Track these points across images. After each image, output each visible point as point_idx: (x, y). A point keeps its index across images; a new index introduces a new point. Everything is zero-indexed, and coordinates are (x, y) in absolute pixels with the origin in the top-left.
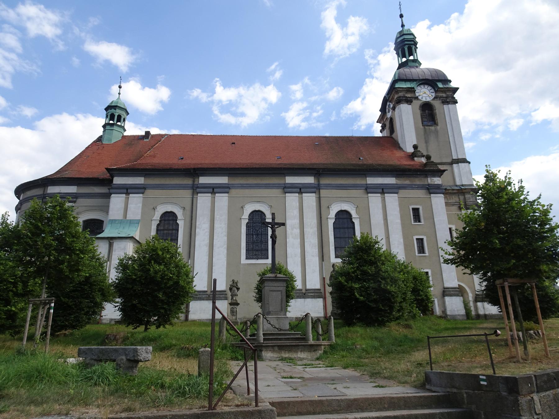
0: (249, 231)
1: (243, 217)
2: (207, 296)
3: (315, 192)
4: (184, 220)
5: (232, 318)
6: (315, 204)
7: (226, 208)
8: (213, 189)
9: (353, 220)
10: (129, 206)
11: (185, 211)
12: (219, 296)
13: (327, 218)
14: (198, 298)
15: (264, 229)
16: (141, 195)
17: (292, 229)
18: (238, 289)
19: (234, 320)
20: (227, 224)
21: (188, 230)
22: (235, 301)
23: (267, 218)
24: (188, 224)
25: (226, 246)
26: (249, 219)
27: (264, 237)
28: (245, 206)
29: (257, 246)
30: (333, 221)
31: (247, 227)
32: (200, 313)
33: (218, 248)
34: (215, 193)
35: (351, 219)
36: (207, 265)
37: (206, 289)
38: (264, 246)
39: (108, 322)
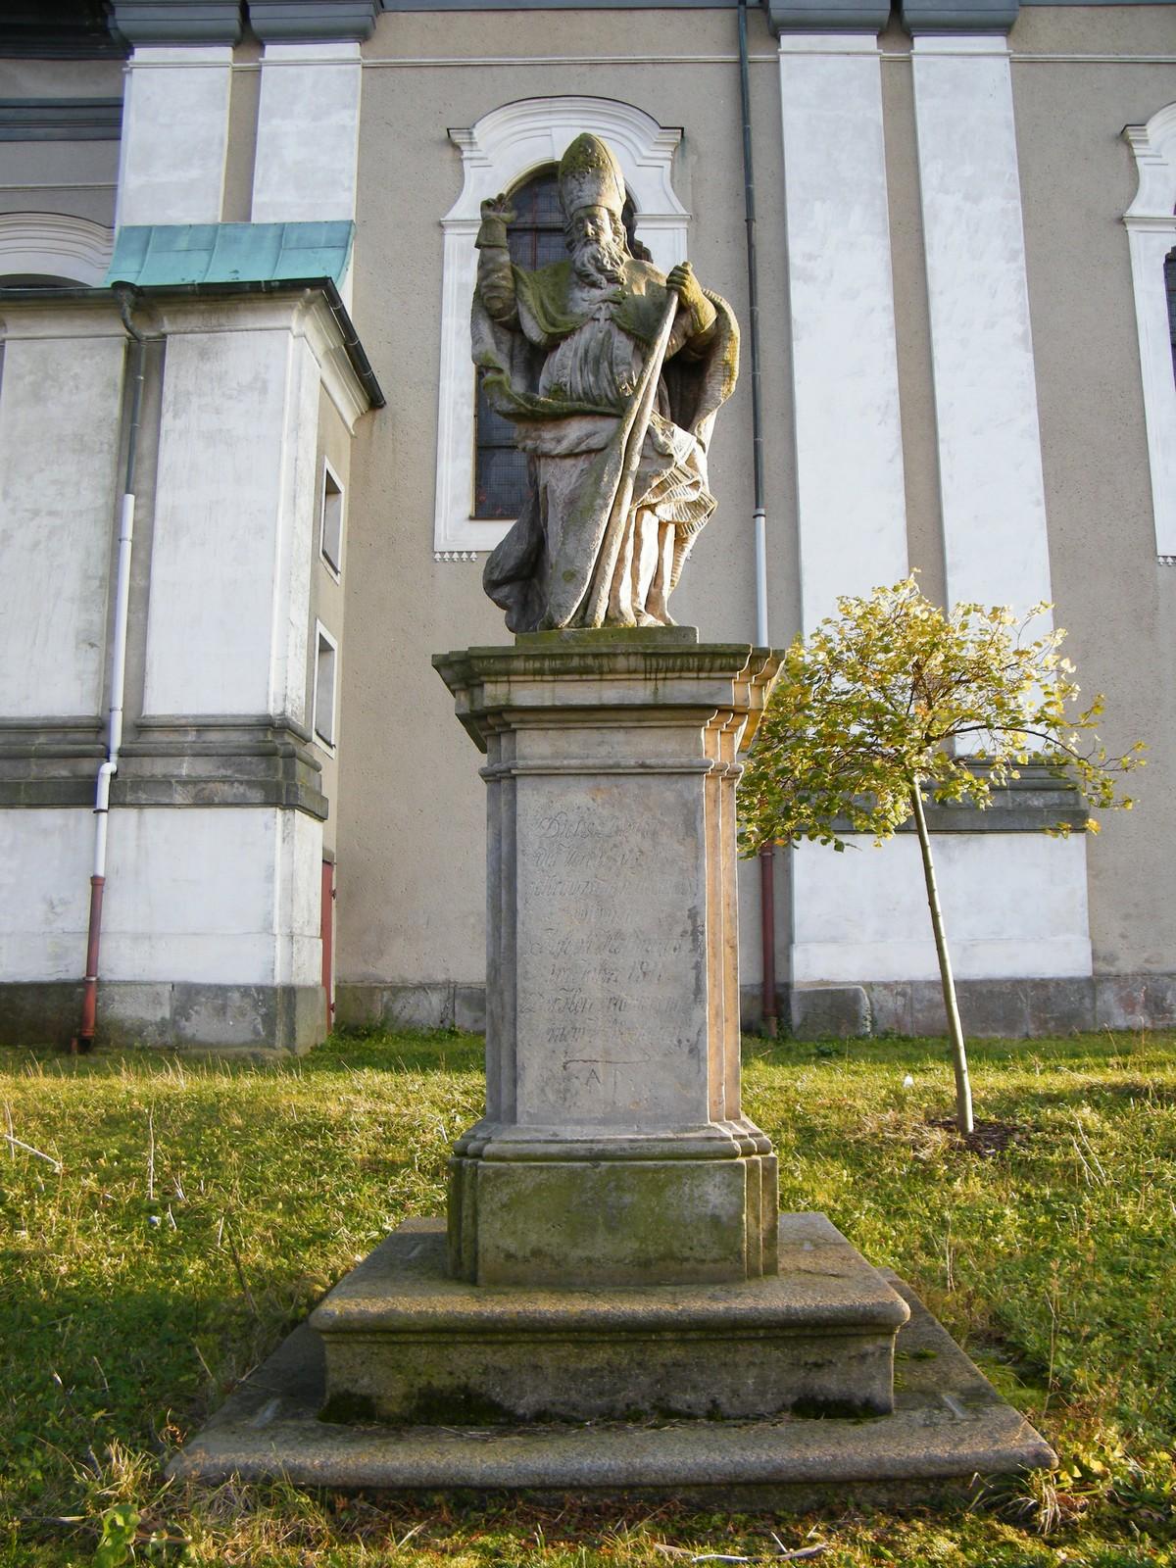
1: (1136, 209)
10: (263, 129)
11: (692, 159)
12: (1020, 797)
16: (350, 50)
20: (1022, 257)
39: (165, 1012)
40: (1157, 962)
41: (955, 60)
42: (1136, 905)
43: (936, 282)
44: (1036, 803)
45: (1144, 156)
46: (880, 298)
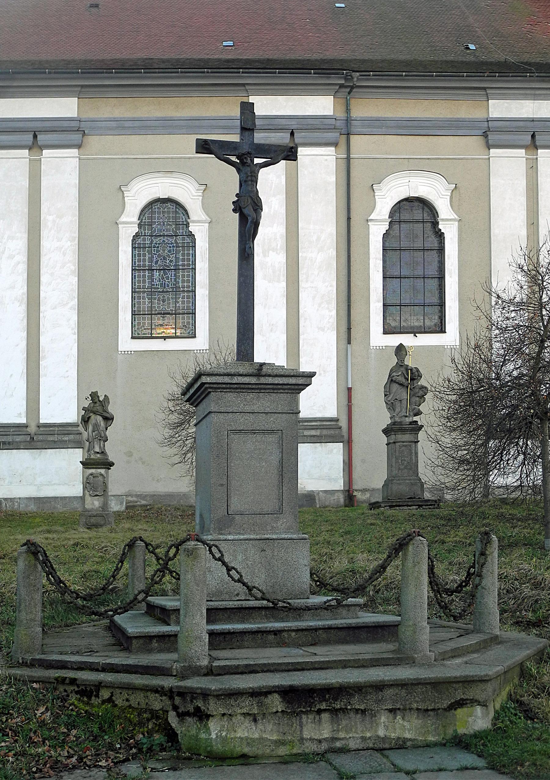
0: (139, 261)
1: (123, 219)
3: (335, 144)
5: (93, 504)
6: (333, 179)
7: (75, 192)
8: (35, 136)
9: (440, 227)
15: (183, 255)
18: (108, 419)
19: (97, 510)
22: (98, 455)
23: (194, 222)
26: (140, 226)
27: (183, 276)
29: (164, 301)
30: (385, 227)
31: (134, 248)
33: (55, 308)
34: (41, 148)
35: (435, 224)
38: (183, 302)
41: (57, 159)
43: (43, 251)
46: (22, 258)
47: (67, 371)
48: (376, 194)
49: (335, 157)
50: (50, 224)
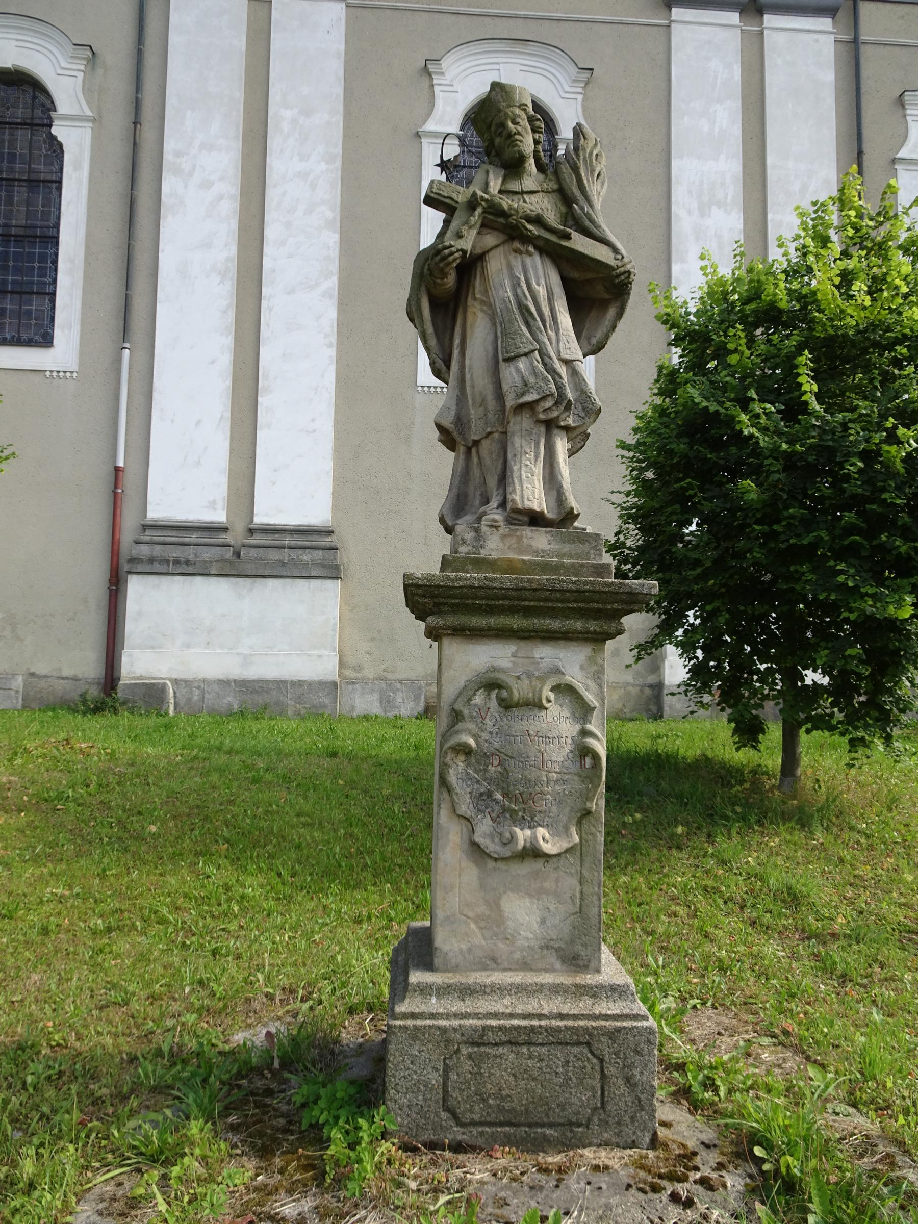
2: (229, 554)
4: (94, 120)
7: (335, 68)
11: (100, 71)
12: (294, 554)
13: (894, 161)
14: (177, 562)
17: (703, 211)
20: (338, 163)
21: (115, 183)
24: (118, 150)
25: (332, 282)
28: (444, 63)
32: (188, 646)
33: (291, 292)
36: (229, 383)
37: (219, 516)
40: (393, 672)
42: (379, 631)
43: (272, 177)
44: (305, 558)
45: (440, 85)
47: (313, 420)
48: (908, 112)
49: (832, 37)
50: (286, 127)
